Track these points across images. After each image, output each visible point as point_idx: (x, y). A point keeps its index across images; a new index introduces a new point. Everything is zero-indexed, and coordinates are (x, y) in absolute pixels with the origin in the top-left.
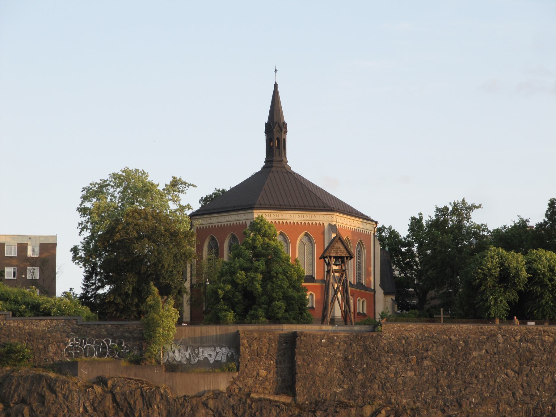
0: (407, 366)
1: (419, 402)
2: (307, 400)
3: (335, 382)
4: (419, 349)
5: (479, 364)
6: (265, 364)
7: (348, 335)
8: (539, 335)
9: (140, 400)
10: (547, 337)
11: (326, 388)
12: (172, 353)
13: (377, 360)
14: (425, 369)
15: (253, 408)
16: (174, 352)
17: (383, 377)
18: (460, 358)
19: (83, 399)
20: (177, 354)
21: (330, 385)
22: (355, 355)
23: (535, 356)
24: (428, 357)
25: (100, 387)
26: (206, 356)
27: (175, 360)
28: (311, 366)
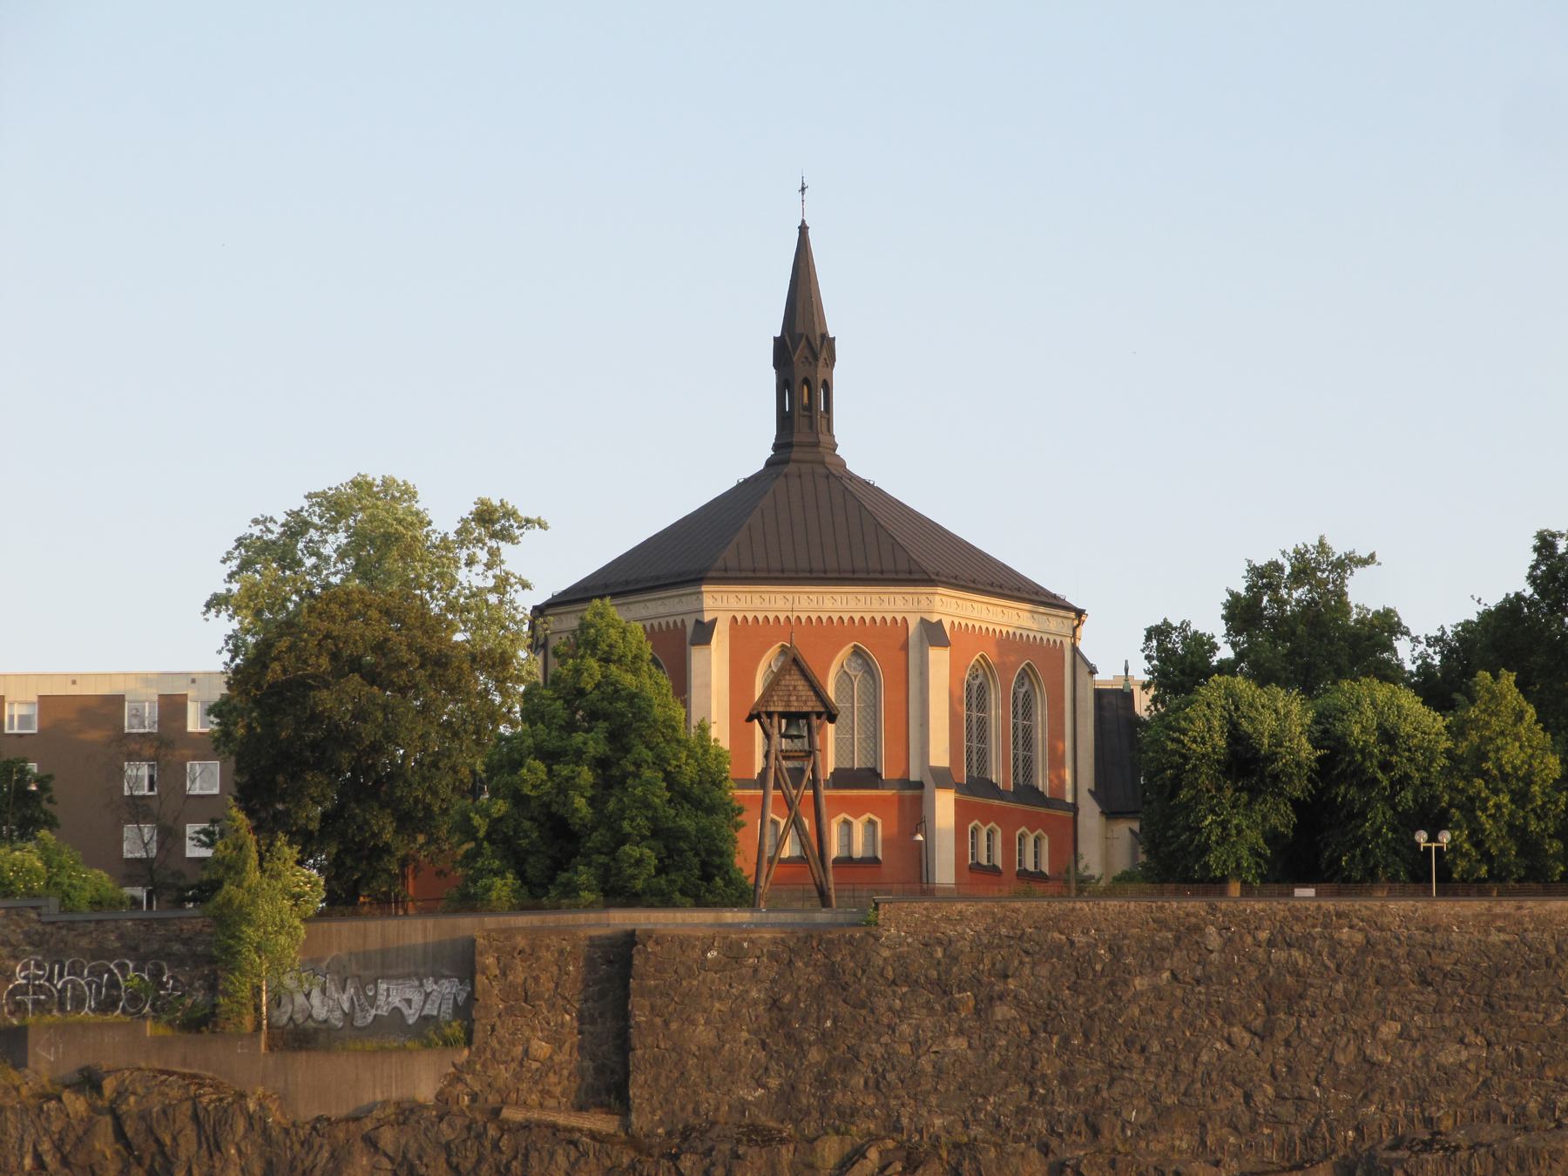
0: (948, 1022)
1: (980, 1125)
2: (661, 1122)
3: (744, 1070)
4: (983, 971)
5: (1152, 1012)
6: (548, 1023)
7: (783, 935)
8: (1325, 926)
9: (190, 1131)
10: (1346, 930)
11: (718, 1088)
12: (303, 997)
13: (863, 1006)
14: (997, 1028)
15: (504, 1148)
16: (308, 996)
17: (879, 1056)
18: (1099, 996)
19: (33, 1131)
20: (316, 998)
21: (729, 1079)
22: (802, 992)
23: (1311, 985)
24: (1008, 995)
25: (82, 1098)
26: (397, 1004)
27: (310, 1016)
28: (674, 1026)
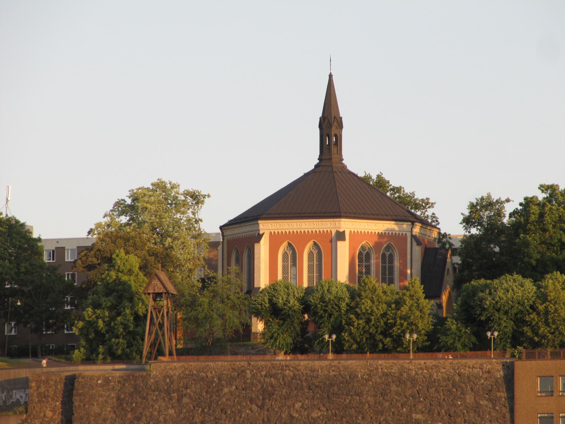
8: (282, 370)
10: (288, 371)
22: (127, 394)
23: (276, 390)
28: (87, 406)
